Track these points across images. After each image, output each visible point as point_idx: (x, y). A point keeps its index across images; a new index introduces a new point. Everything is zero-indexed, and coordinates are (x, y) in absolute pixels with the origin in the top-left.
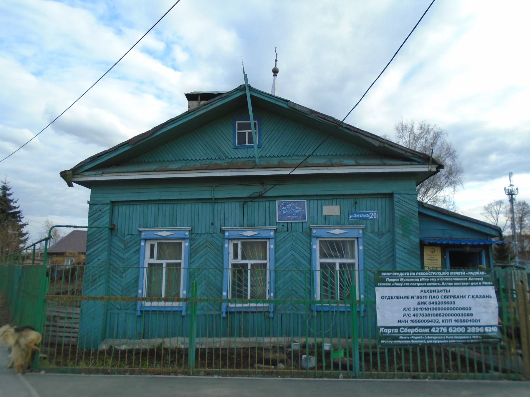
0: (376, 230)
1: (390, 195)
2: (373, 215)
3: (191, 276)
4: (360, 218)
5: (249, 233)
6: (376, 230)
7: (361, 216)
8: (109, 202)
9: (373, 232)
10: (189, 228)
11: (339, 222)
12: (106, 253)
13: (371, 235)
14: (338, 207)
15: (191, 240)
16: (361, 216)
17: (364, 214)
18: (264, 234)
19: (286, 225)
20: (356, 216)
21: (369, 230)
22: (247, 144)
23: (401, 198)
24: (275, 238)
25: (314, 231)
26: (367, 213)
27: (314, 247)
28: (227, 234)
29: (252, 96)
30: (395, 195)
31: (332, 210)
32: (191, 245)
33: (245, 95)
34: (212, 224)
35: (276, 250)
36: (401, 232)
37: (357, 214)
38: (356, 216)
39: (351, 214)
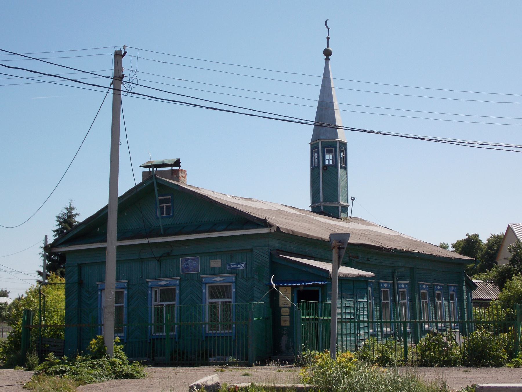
0: (245, 277)
1: (252, 250)
2: (243, 266)
3: (129, 314)
4: (234, 268)
5: (163, 283)
6: (245, 277)
7: (235, 266)
8: (76, 264)
9: (243, 278)
10: (127, 281)
11: (221, 271)
12: (77, 301)
13: (242, 280)
14: (220, 260)
15: (128, 288)
16: (235, 266)
17: (237, 265)
18: (172, 283)
19: (187, 275)
20: (232, 266)
21: (240, 277)
22: (165, 215)
23: (258, 252)
24: (180, 285)
25: (203, 280)
26: (239, 264)
27: (234, 290)
28: (150, 284)
29: (157, 182)
30: (255, 251)
31: (216, 263)
32: (128, 292)
33: (153, 183)
34: (141, 277)
35: (180, 294)
36: (257, 277)
37: (233, 265)
38: (232, 266)
39: (229, 265)
